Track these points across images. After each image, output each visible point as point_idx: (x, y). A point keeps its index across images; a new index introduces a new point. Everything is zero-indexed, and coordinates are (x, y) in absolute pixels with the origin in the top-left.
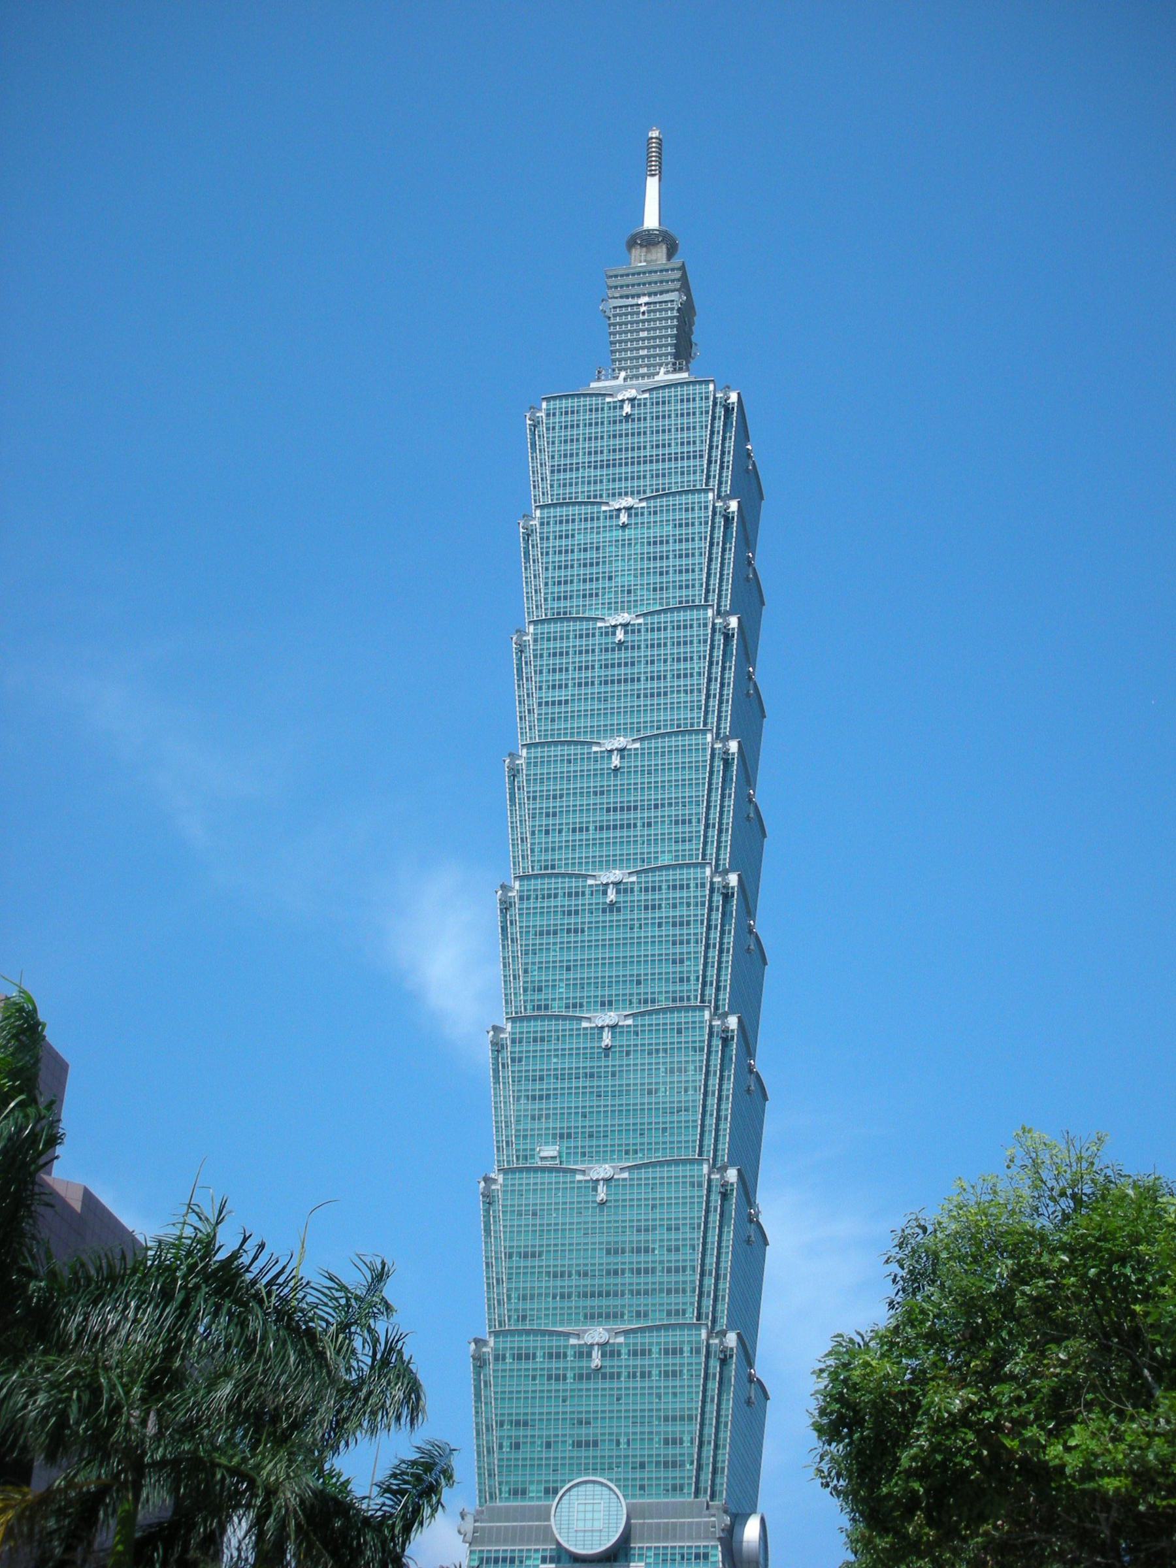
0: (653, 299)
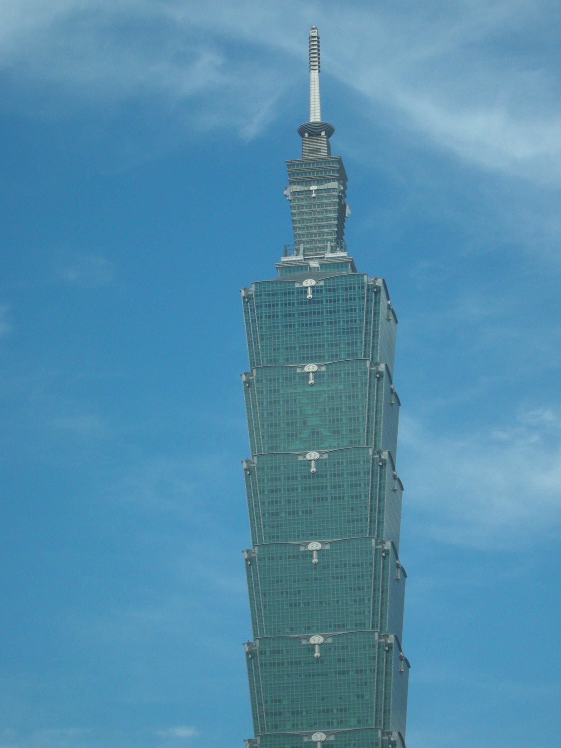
0: (322, 187)
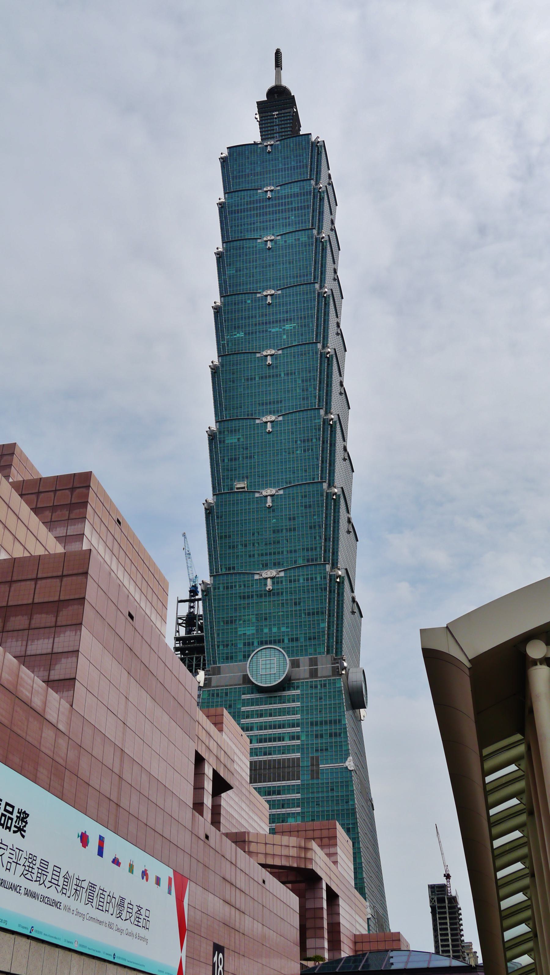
0: (281, 112)
